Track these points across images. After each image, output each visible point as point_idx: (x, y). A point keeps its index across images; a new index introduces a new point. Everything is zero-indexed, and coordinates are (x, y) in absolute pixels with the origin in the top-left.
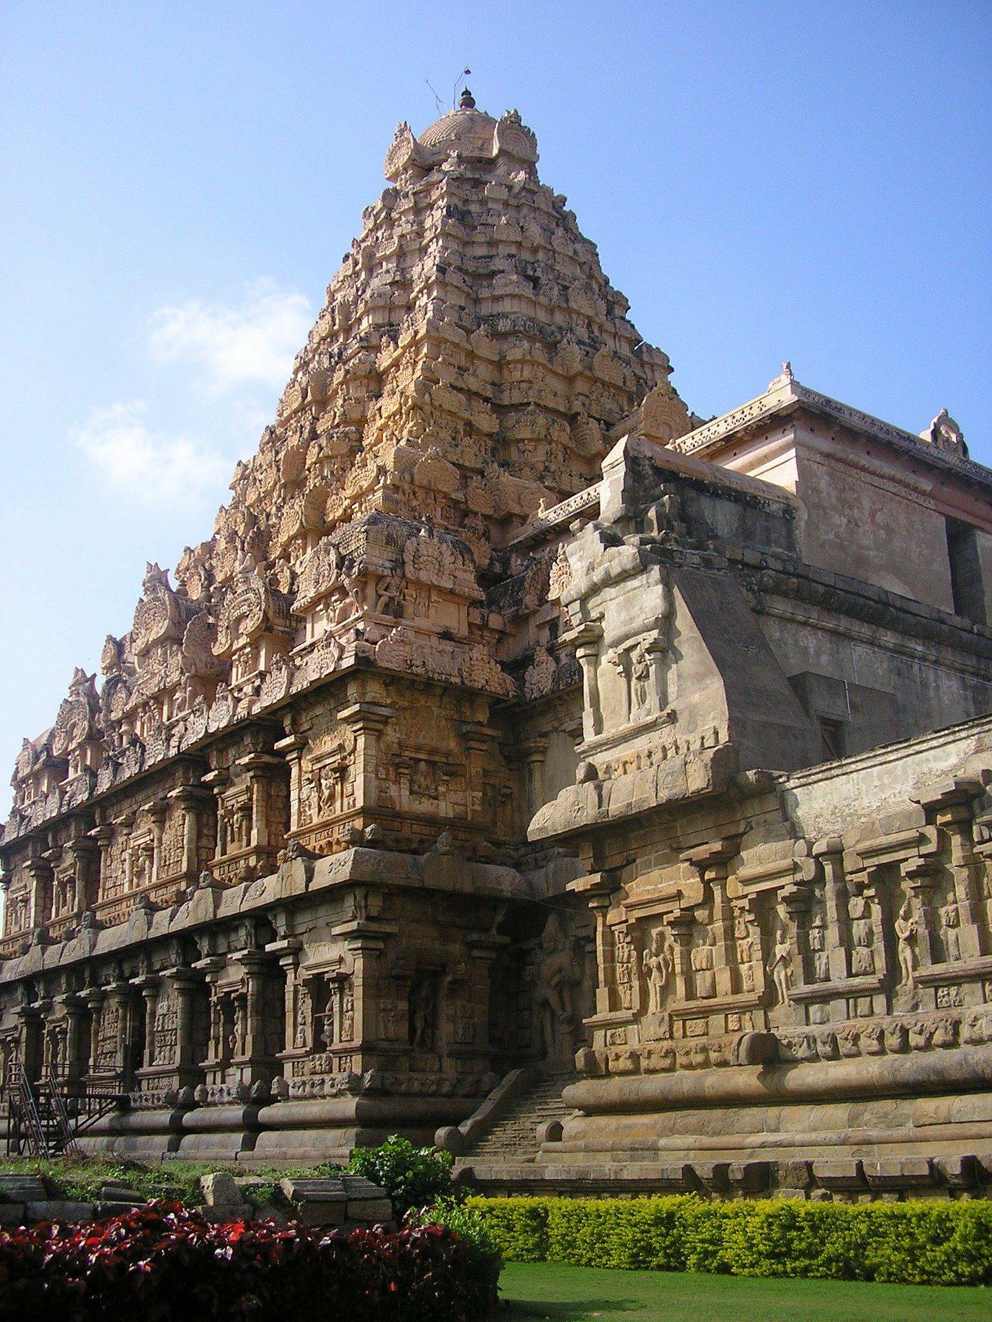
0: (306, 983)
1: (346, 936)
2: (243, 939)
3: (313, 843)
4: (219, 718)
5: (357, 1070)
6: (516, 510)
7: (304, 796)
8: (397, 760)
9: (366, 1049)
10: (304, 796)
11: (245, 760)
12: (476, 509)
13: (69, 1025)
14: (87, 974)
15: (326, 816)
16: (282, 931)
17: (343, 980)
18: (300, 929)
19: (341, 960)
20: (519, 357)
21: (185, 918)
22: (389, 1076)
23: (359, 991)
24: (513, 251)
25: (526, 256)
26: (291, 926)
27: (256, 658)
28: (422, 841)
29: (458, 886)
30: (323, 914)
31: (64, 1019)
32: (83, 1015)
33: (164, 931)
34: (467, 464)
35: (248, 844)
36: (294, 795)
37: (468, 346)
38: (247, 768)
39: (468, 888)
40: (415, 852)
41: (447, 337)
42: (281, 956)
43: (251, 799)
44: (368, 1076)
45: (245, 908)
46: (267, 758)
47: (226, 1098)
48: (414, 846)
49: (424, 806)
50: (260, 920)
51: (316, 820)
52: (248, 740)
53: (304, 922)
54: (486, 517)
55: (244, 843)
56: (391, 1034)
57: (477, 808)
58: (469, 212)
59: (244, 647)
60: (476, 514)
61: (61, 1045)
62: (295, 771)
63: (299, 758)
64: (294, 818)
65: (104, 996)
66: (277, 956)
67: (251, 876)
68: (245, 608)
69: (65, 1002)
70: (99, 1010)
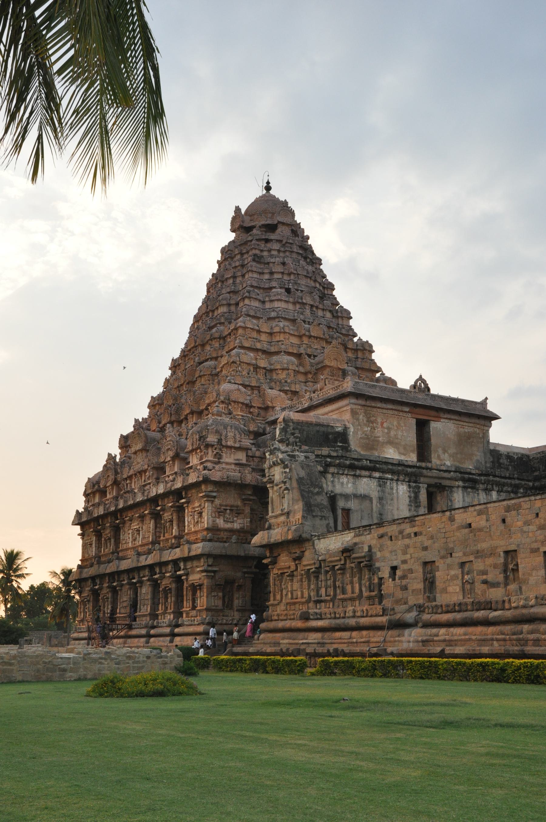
0: (190, 586)
1: (202, 571)
2: (170, 569)
3: (192, 538)
4: (161, 489)
5: (204, 617)
6: (270, 404)
7: (189, 520)
9: (207, 610)
10: (189, 520)
11: (170, 505)
12: (254, 405)
13: (110, 595)
14: (116, 577)
15: (197, 529)
16: (182, 567)
17: (201, 585)
18: (188, 567)
19: (200, 579)
20: (278, 330)
21: (150, 560)
22: (214, 618)
23: (205, 590)
26: (185, 566)
27: (174, 466)
28: (227, 538)
29: (239, 554)
30: (195, 563)
31: (107, 593)
32: (114, 591)
33: (143, 564)
34: (253, 385)
35: (172, 534)
36: (186, 519)
37: (257, 328)
38: (171, 507)
39: (242, 554)
40: (225, 542)
41: (248, 326)
42: (182, 576)
43: (172, 518)
44: (207, 618)
45: (170, 559)
46: (177, 504)
47: (165, 625)
48: (225, 540)
49: (229, 526)
50: (175, 562)
51: (193, 529)
52: (171, 497)
53: (189, 565)
54: (259, 408)
55: (170, 534)
56: (216, 605)
57: (248, 524)
58: (262, 256)
59: (169, 461)
60: (255, 407)
61: (106, 603)
62: (186, 511)
63: (188, 506)
64: (186, 527)
65: (122, 585)
66: (180, 576)
67: (172, 547)
68: (169, 447)
69: (108, 587)
70: (121, 590)
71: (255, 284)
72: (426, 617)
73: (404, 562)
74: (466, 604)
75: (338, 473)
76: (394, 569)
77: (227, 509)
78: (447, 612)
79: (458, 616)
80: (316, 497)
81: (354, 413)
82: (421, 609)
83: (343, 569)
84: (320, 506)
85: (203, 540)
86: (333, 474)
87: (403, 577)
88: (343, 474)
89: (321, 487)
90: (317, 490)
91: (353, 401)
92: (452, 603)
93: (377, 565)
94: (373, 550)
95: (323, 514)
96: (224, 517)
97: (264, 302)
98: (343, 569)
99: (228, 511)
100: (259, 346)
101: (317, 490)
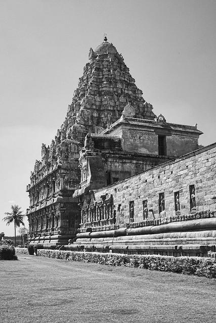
24: (107, 76)
25: (110, 77)
71: (95, 80)
72: (129, 230)
73: (123, 202)
74: (144, 223)
75: (113, 162)
76: (120, 205)
78: (138, 227)
79: (140, 229)
80: (99, 173)
81: (124, 133)
82: (128, 226)
83: (102, 207)
84: (100, 177)
85: (60, 195)
86: (111, 162)
87: (123, 210)
88: (116, 162)
89: (103, 168)
91: (124, 127)
92: (139, 222)
93: (114, 204)
94: (113, 197)
95: (102, 181)
97: (99, 88)
98: (102, 207)
100: (94, 107)
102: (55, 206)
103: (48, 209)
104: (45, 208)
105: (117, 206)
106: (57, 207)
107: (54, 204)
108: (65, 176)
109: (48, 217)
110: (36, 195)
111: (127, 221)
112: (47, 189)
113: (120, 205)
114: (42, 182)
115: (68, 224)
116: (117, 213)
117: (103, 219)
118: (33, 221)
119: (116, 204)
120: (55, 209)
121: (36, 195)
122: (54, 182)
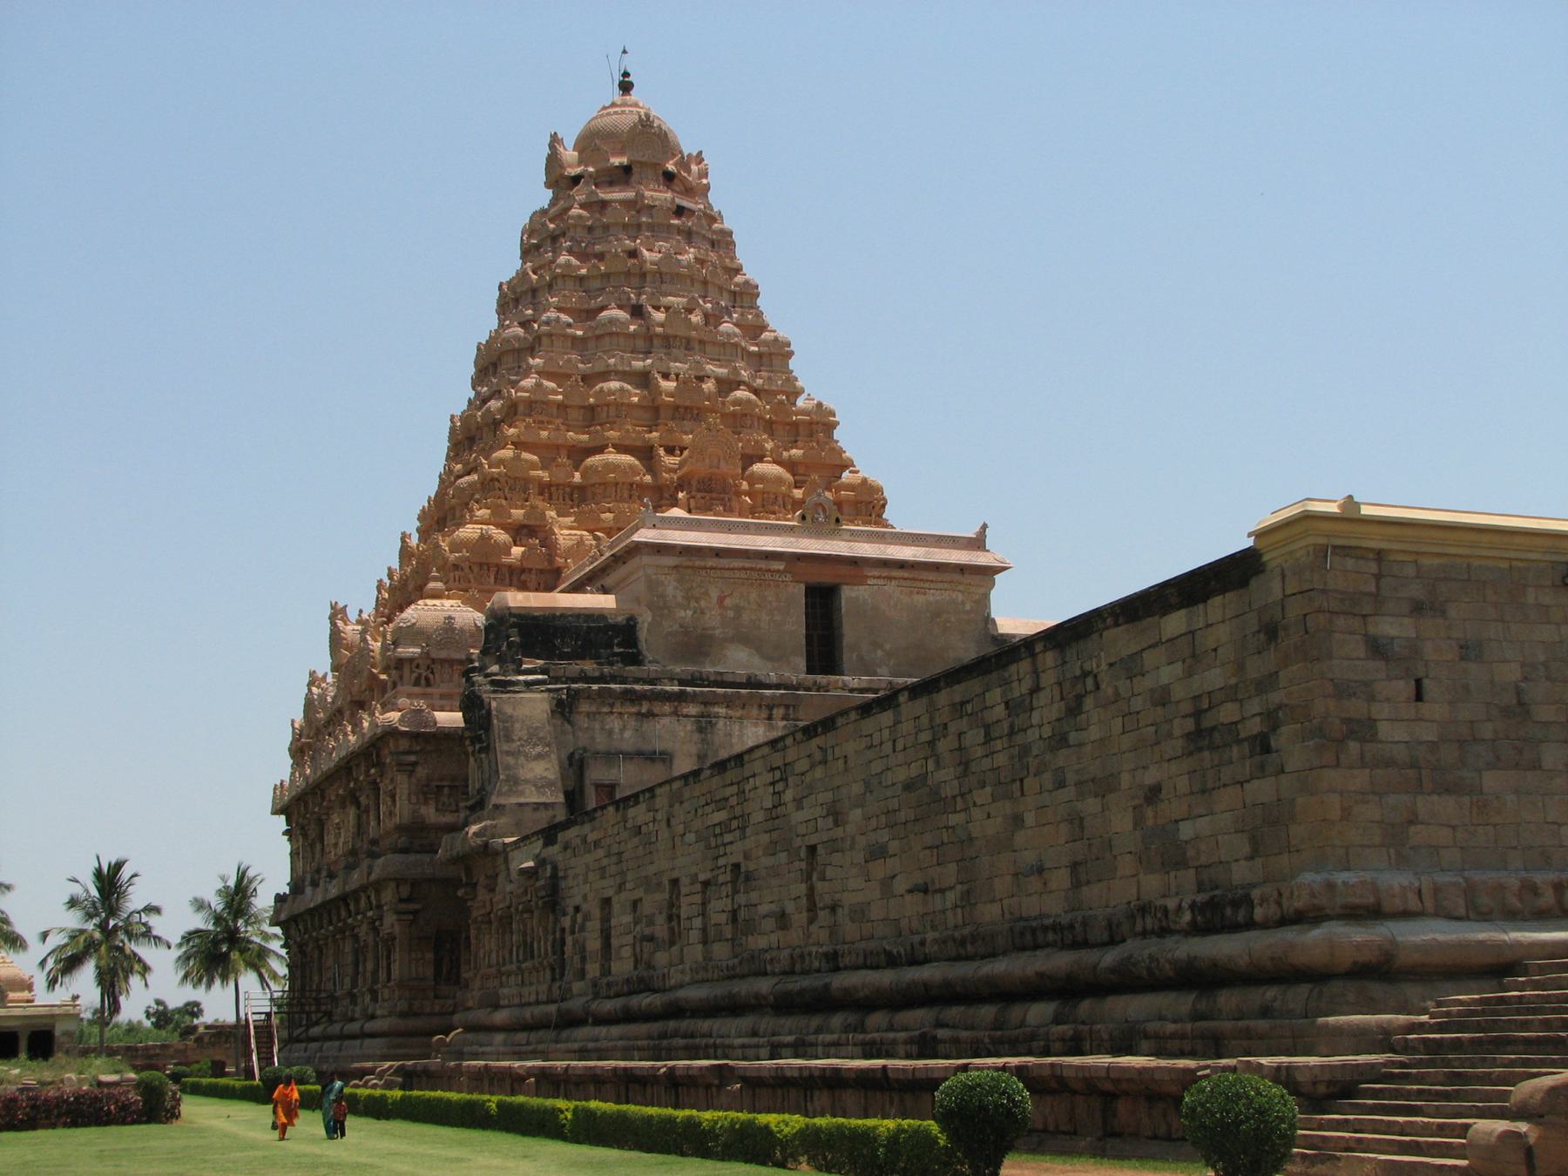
8: (425, 789)
77: (444, 786)
90: (539, 749)
96: (437, 802)
99: (446, 791)
101: (539, 749)
102: (378, 892)
103: (357, 901)
104: (343, 899)
105: (571, 910)
106: (388, 895)
107: (378, 886)
108: (414, 764)
109: (356, 937)
110: (313, 834)
111: (593, 969)
112: (352, 812)
113: (577, 909)
114: (331, 777)
115: (430, 972)
116: (569, 940)
117: (532, 957)
118: (303, 953)
119: (570, 904)
120: (379, 907)
121: (313, 834)
122: (375, 787)
